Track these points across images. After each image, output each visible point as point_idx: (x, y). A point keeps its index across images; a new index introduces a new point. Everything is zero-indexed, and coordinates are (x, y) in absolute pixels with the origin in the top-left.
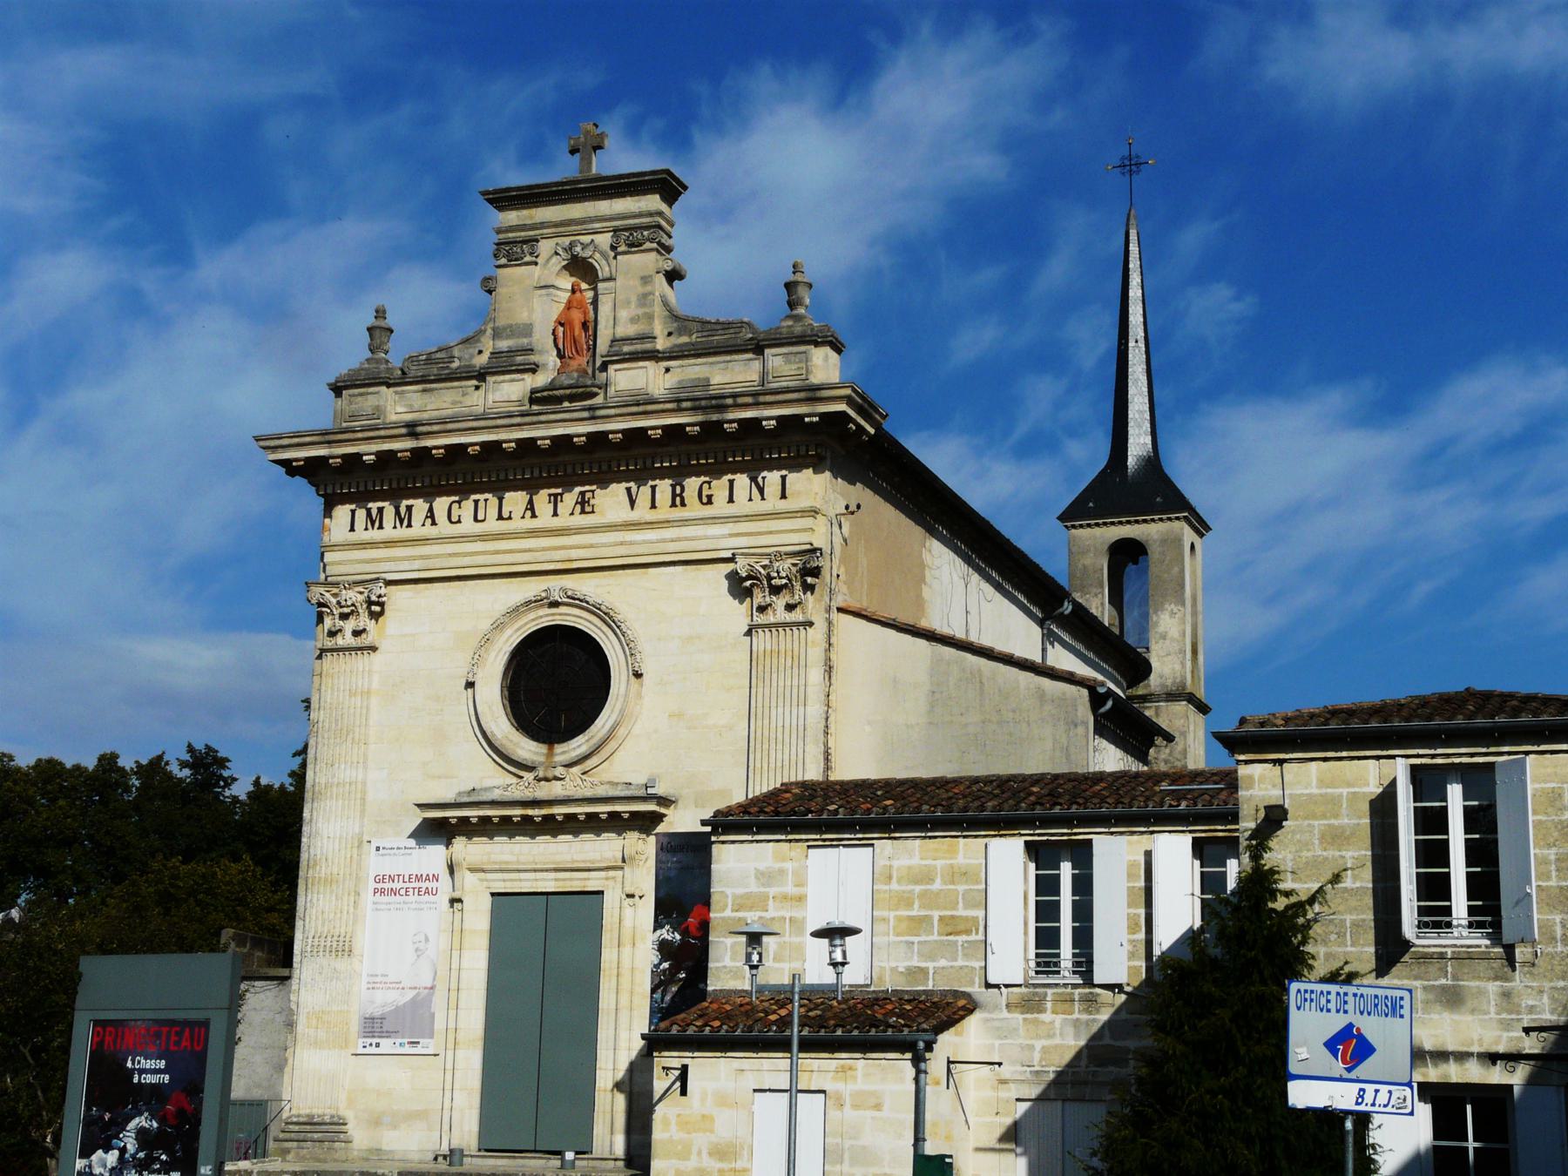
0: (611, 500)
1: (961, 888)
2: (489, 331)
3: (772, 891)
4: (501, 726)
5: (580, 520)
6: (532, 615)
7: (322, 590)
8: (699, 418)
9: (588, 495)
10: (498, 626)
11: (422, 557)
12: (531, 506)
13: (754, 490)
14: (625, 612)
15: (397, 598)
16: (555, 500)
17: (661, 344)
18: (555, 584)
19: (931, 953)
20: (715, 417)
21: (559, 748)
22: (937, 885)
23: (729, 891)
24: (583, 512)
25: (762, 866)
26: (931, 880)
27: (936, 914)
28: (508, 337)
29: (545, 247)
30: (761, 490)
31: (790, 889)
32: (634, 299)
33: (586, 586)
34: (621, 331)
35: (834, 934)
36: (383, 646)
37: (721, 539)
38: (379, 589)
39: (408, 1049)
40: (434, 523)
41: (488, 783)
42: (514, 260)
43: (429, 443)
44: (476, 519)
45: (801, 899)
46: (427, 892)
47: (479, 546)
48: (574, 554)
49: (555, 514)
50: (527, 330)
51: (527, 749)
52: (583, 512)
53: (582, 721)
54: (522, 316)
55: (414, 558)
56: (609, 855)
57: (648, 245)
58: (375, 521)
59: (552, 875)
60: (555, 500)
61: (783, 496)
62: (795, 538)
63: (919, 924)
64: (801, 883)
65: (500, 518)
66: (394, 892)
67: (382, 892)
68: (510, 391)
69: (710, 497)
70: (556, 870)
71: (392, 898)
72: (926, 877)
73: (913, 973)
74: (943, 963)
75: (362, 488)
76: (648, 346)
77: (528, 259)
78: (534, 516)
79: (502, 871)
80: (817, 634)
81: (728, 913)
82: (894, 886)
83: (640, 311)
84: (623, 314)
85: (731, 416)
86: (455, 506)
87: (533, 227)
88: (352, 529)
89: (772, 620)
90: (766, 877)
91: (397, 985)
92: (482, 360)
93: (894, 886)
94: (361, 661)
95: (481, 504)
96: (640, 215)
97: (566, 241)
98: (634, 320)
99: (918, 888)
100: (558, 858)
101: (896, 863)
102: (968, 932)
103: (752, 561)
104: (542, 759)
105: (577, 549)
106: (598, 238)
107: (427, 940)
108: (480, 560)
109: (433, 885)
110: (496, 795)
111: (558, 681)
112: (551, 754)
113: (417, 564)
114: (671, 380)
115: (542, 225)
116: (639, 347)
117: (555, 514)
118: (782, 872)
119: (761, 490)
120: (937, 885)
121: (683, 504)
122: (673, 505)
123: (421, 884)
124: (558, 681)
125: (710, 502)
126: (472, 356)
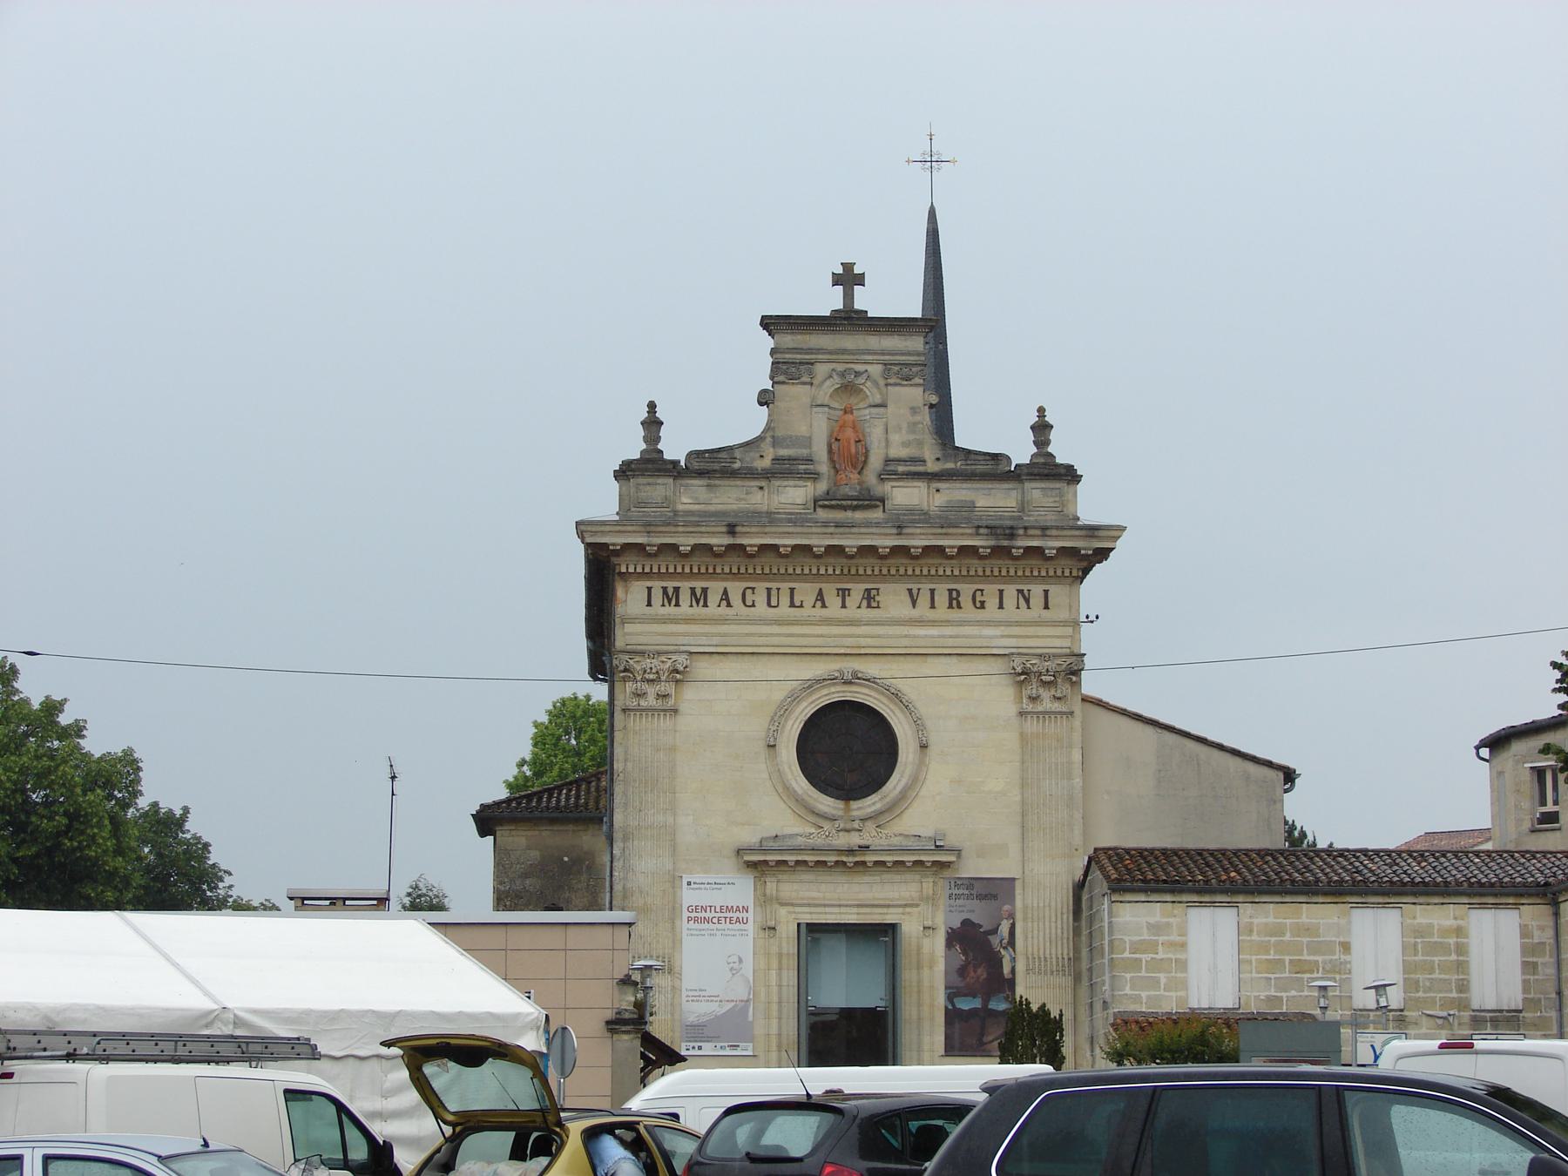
0: (894, 599)
1: (1305, 940)
2: (769, 440)
3: (1161, 939)
4: (801, 784)
5: (865, 613)
6: (825, 692)
7: (626, 657)
8: (992, 543)
9: (873, 592)
10: (794, 698)
11: (719, 635)
12: (820, 596)
13: (1021, 600)
14: (908, 689)
15: (703, 668)
16: (844, 593)
17: (932, 467)
18: (850, 665)
19: (1283, 985)
20: (1006, 543)
21: (854, 804)
22: (1287, 937)
23: (1127, 939)
24: (869, 606)
25: (1152, 920)
26: (1283, 934)
27: (1287, 958)
28: (788, 447)
29: (821, 370)
30: (1027, 601)
31: (1175, 938)
32: (905, 426)
33: (871, 668)
34: (896, 452)
35: (1380, 989)
36: (683, 707)
37: (997, 637)
38: (682, 659)
39: (728, 1052)
40: (729, 605)
41: (788, 831)
42: (793, 378)
43: (745, 541)
44: (769, 605)
45: (1183, 945)
46: (738, 920)
47: (776, 629)
48: (863, 641)
49: (844, 606)
50: (807, 441)
51: (826, 803)
52: (869, 606)
53: (875, 783)
54: (802, 430)
55: (713, 635)
56: (907, 894)
57: (918, 380)
58: (672, 597)
59: (855, 910)
60: (844, 593)
61: (1046, 607)
62: (1058, 643)
63: (1276, 965)
64: (1183, 933)
65: (792, 605)
66: (708, 920)
67: (696, 920)
68: (795, 495)
69: (983, 603)
70: (859, 906)
71: (706, 926)
72: (1278, 931)
73: (1269, 999)
74: (1293, 993)
75: (647, 570)
76: (921, 469)
77: (805, 379)
78: (824, 606)
79: (809, 905)
80: (1077, 723)
81: (1127, 955)
82: (1255, 937)
83: (911, 437)
84: (895, 438)
85: (1020, 543)
86: (749, 592)
87: (810, 351)
88: (649, 604)
89: (1040, 709)
90: (1156, 928)
91: (711, 998)
92: (766, 463)
93: (1255, 937)
94: (665, 723)
95: (774, 593)
96: (909, 354)
97: (840, 367)
98: (905, 444)
99: (1273, 939)
100: (861, 896)
101: (1256, 921)
102: (1311, 972)
103: (1024, 659)
104: (841, 813)
105: (865, 637)
106: (870, 368)
107: (741, 961)
108: (775, 640)
109: (745, 915)
110: (800, 841)
111: (848, 748)
112: (848, 809)
113: (715, 640)
114: (939, 500)
115: (819, 351)
116: (913, 469)
117: (844, 606)
118: (1168, 925)
119: (1027, 601)
120: (1287, 937)
121: (959, 607)
122: (950, 606)
123: (731, 914)
124: (848, 748)
125: (982, 606)
126: (753, 460)
